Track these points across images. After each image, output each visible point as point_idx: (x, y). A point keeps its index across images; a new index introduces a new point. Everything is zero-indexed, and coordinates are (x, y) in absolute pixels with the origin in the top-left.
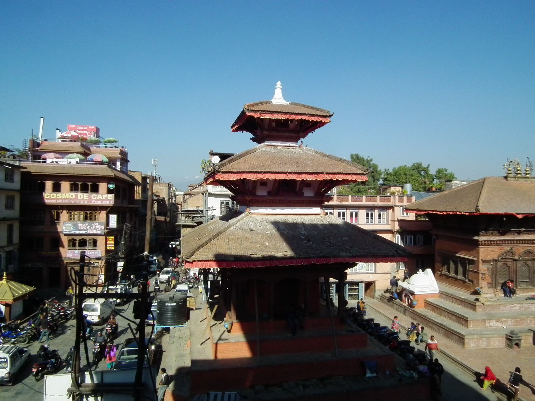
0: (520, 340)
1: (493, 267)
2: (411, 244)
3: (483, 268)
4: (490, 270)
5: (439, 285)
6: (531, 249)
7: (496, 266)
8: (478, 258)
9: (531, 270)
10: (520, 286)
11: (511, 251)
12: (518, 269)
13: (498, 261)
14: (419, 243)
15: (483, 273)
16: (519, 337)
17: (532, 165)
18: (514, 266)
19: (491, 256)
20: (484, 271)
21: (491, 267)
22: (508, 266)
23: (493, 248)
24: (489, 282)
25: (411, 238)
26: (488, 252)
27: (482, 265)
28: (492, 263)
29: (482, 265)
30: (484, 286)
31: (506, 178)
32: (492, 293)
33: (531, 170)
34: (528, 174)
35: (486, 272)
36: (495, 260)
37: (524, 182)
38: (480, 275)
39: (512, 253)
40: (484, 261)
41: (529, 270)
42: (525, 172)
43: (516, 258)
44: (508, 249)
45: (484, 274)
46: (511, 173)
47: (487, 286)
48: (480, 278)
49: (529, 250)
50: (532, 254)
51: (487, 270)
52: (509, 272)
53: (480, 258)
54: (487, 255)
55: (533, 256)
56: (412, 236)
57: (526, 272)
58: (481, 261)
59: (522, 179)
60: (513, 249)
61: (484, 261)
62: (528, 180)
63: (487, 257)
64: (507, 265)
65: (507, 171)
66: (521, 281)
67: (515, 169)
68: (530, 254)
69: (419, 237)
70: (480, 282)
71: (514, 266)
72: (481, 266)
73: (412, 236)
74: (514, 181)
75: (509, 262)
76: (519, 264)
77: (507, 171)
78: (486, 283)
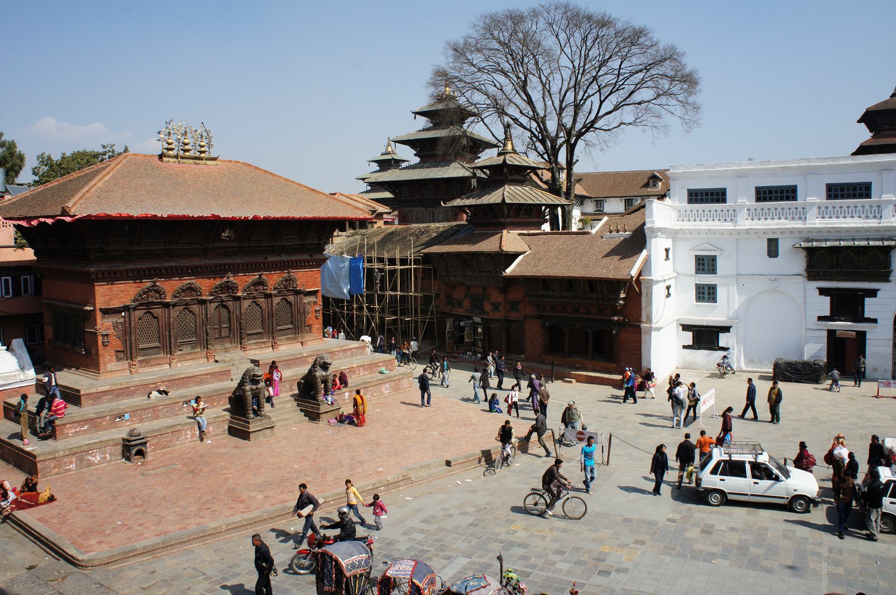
0: (146, 443)
1: (125, 321)
2: (7, 293)
3: (104, 325)
4: (120, 326)
5: (36, 367)
6: (192, 283)
7: (130, 318)
8: (94, 306)
9: (198, 321)
10: (180, 350)
11: (156, 288)
12: (171, 320)
13: (135, 309)
14: (26, 292)
15: (104, 333)
16: (143, 438)
17: (212, 137)
18: (166, 316)
19: (121, 300)
20: (108, 329)
21: (122, 320)
22: (156, 318)
23: (122, 285)
24: (118, 349)
25: (6, 281)
26: (113, 292)
27: (103, 318)
28: (123, 314)
29: (103, 318)
30: (109, 357)
31: (161, 157)
32: (125, 369)
33: (209, 145)
34: (204, 152)
35: (111, 332)
36: (126, 308)
37: (193, 166)
38: (100, 339)
39: (157, 291)
40: (106, 312)
41: (195, 321)
43: (168, 300)
44: (149, 284)
45: (107, 335)
47: (115, 357)
48: (100, 343)
49: (189, 286)
51: (112, 327)
52: (159, 326)
53: (98, 306)
54: (111, 300)
55: (200, 295)
56: (10, 278)
57: (191, 324)
58: (99, 314)
59: (192, 161)
60: (158, 284)
61: (106, 312)
62: (201, 162)
63: (111, 303)
64: (152, 315)
65: (166, 146)
66: (182, 341)
67: (179, 143)
68: (193, 292)
69: (25, 280)
70: (100, 352)
71: (166, 316)
72: (99, 321)
73: (10, 278)
74: (175, 162)
75: (157, 310)
76: (174, 313)
77: (166, 146)
78: (113, 353)
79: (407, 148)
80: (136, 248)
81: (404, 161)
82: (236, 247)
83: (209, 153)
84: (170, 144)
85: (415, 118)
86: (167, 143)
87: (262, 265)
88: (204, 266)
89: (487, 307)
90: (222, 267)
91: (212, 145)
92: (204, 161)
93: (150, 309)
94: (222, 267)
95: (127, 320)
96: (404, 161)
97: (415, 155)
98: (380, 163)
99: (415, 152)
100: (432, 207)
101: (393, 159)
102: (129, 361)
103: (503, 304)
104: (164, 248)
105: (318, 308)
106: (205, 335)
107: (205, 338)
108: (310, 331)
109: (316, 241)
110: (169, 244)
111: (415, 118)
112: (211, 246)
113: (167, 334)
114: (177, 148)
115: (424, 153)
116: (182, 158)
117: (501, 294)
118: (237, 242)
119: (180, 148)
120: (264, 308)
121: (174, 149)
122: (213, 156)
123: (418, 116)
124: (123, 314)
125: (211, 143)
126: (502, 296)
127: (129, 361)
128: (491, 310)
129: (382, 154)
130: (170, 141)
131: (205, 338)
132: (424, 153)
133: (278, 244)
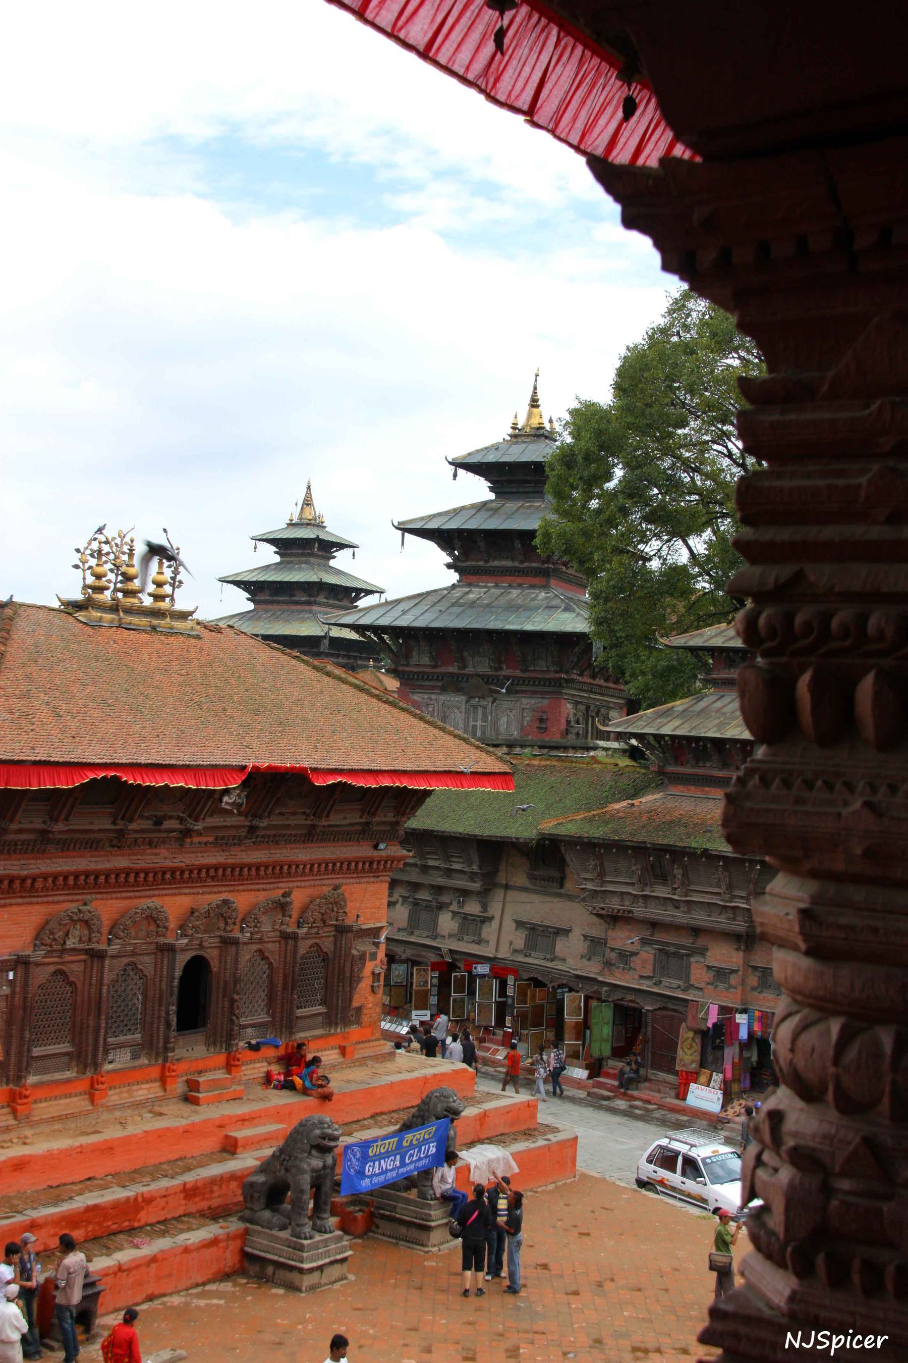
22: (72, 984)
28: (11, 975)
33: (175, 583)
42: (151, 588)
46: (101, 589)
50: (158, 926)
57: (136, 1001)
65: (90, 580)
67: (117, 575)
77: (90, 580)
79: (430, 548)
80: (60, 826)
81: (342, 546)
82: (244, 827)
83: (173, 600)
84: (99, 577)
85: (455, 476)
86: (93, 575)
87: (286, 868)
88: (178, 869)
89: (698, 974)
90: (212, 872)
91: (181, 582)
92: (168, 620)
93: (63, 963)
94: (212, 872)
95: (18, 989)
96: (342, 546)
97: (449, 566)
98: (283, 545)
99: (449, 560)
100: (483, 697)
101: (318, 539)
102: (11, 1086)
103: (740, 973)
104: (113, 827)
105: (377, 971)
106: (162, 1028)
107: (161, 1034)
108: (359, 1022)
109: (390, 818)
110: (122, 819)
111: (455, 476)
112: (199, 826)
113: (91, 1023)
114: (112, 586)
115: (469, 563)
116: (129, 611)
117: (738, 949)
118: (246, 816)
119: (119, 585)
120: (275, 965)
121: (107, 588)
122: (180, 605)
123: (461, 472)
124: (11, 975)
125: (178, 578)
126: (741, 954)
127: (11, 1086)
128: (708, 984)
129: (291, 525)
130: (99, 570)
131: (161, 1034)
132: (469, 563)
133: (323, 822)
